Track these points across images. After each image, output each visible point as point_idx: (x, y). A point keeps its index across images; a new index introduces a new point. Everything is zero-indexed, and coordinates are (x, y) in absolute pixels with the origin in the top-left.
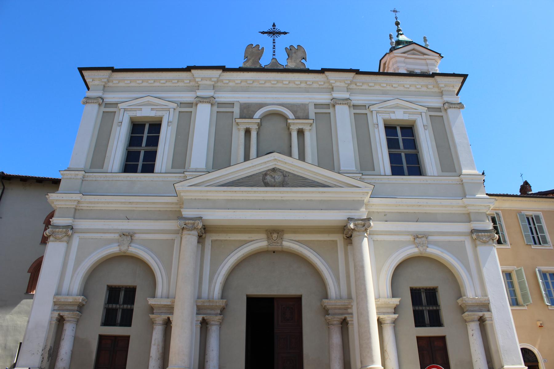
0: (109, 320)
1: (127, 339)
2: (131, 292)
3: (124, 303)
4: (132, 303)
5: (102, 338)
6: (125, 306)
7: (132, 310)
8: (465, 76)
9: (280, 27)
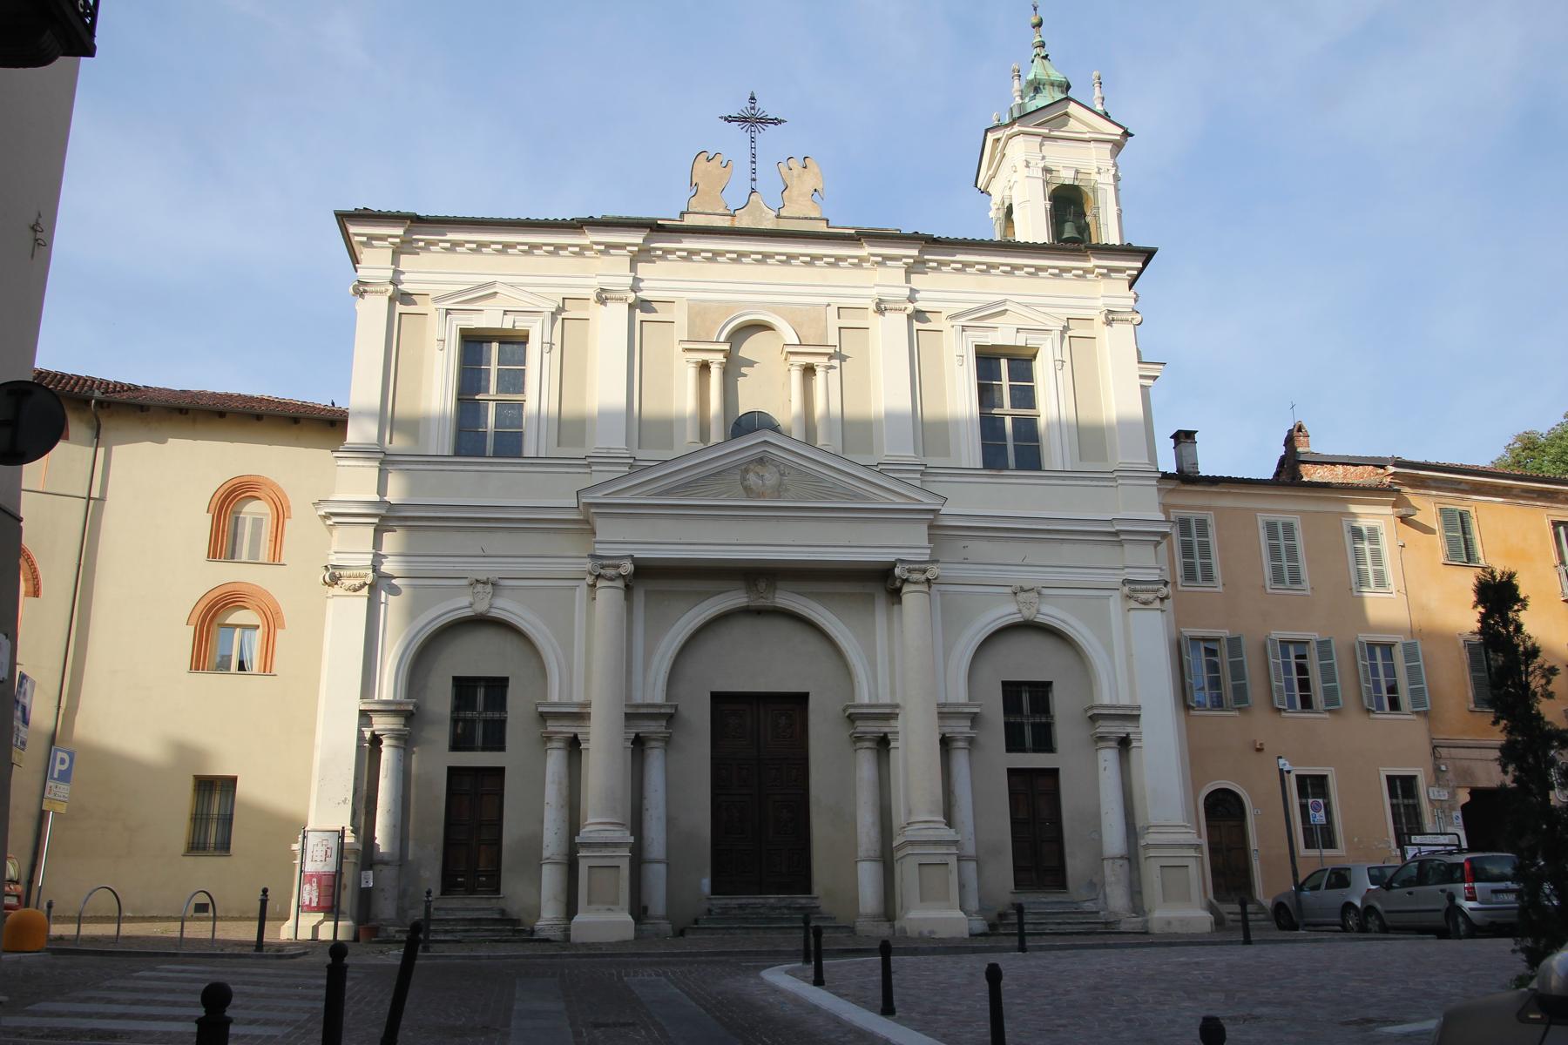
1: (499, 772)
2: (497, 687)
3: (486, 709)
4: (502, 705)
5: (452, 771)
6: (489, 715)
7: (503, 722)
8: (1148, 255)
9: (767, 108)
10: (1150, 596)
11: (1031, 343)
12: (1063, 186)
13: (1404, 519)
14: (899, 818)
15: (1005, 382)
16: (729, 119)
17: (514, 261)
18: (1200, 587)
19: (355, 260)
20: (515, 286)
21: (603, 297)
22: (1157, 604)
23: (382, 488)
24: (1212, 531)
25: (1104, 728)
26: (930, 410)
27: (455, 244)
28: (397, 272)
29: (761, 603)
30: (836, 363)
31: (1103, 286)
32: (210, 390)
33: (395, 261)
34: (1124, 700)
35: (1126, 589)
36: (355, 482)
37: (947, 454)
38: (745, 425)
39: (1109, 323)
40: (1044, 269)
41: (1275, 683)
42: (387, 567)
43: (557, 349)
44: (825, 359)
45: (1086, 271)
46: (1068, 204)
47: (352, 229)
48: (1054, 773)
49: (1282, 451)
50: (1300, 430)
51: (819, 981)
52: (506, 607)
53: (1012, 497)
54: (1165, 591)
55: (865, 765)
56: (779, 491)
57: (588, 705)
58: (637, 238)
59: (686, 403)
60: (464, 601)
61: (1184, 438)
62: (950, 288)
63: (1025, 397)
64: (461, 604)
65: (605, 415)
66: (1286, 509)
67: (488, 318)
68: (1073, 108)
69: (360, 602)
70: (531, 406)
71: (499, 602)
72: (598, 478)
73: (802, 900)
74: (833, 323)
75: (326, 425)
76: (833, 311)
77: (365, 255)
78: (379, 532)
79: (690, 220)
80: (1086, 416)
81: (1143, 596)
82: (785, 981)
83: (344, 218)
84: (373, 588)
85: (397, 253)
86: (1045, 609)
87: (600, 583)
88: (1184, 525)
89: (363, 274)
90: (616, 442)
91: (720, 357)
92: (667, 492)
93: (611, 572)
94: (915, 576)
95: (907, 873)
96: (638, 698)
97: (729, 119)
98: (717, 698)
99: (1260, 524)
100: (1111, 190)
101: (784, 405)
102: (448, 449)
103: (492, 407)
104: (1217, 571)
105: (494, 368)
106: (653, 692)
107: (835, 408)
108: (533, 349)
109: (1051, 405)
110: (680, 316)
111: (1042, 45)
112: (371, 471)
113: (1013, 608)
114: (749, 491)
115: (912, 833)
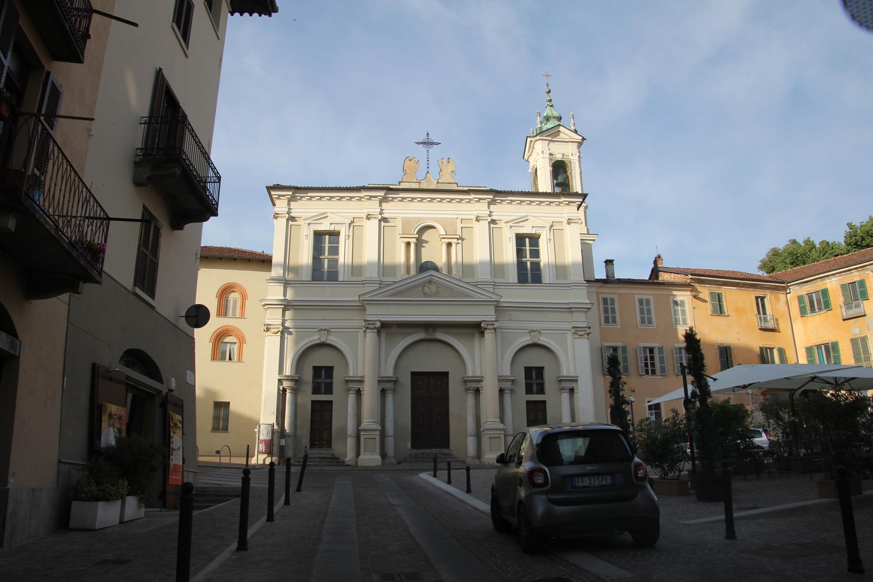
0: (316, 391)
1: (330, 403)
2: (329, 370)
4: (332, 378)
5: (314, 403)
6: (327, 381)
7: (331, 384)
9: (433, 138)
10: (583, 333)
11: (538, 232)
12: (558, 161)
13: (695, 297)
14: (483, 421)
15: (528, 248)
16: (418, 143)
17: (335, 203)
18: (611, 326)
19: (274, 205)
20: (335, 213)
21: (368, 217)
22: (586, 336)
23: (285, 294)
24: (616, 303)
25: (564, 385)
26: (497, 260)
27: (312, 197)
28: (290, 209)
29: (431, 337)
30: (460, 241)
31: (567, 208)
32: (215, 245)
33: (289, 205)
34: (572, 374)
35: (573, 330)
36: (276, 293)
37: (503, 277)
38: (425, 267)
39: (569, 223)
40: (543, 202)
41: (640, 364)
42: (287, 324)
43: (351, 238)
44: (455, 240)
45: (560, 203)
46: (559, 168)
47: (273, 193)
48: (545, 402)
49: (652, 266)
50: (659, 257)
51: (435, 476)
52: (333, 340)
53: (530, 294)
54: (588, 331)
55: (470, 399)
56: (437, 294)
57: (363, 377)
58: (381, 194)
59: (401, 259)
60: (316, 337)
61: (609, 262)
62: (505, 211)
63: (535, 253)
64: (315, 339)
65: (370, 264)
66: (648, 294)
67: (324, 226)
68: (561, 129)
69: (278, 338)
70: (341, 261)
71: (330, 338)
72: (367, 290)
73: (445, 451)
74: (459, 225)
75: (263, 261)
76: (459, 221)
77: (277, 202)
78: (284, 311)
79: (404, 186)
80: (560, 261)
81: (580, 333)
82: (426, 476)
83: (269, 189)
84: (282, 333)
85: (289, 201)
86: (542, 338)
87: (368, 331)
88: (605, 300)
89: (277, 210)
90: (374, 275)
91: (414, 240)
92: (393, 295)
93: (372, 326)
94: (490, 327)
95: (485, 440)
96: (383, 374)
97: (418, 143)
98: (413, 374)
99: (636, 300)
100: (577, 162)
101: (440, 260)
102: (309, 278)
103: (326, 260)
104: (618, 319)
105: (327, 245)
106: (389, 372)
107: (460, 260)
108: (342, 238)
109: (546, 257)
110: (399, 224)
111: (550, 101)
112: (280, 288)
113: (529, 338)
114: (425, 294)
115: (487, 426)
